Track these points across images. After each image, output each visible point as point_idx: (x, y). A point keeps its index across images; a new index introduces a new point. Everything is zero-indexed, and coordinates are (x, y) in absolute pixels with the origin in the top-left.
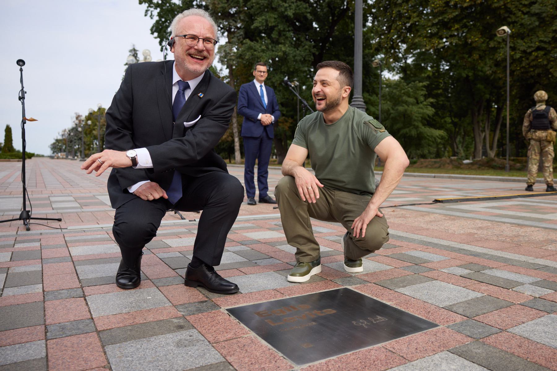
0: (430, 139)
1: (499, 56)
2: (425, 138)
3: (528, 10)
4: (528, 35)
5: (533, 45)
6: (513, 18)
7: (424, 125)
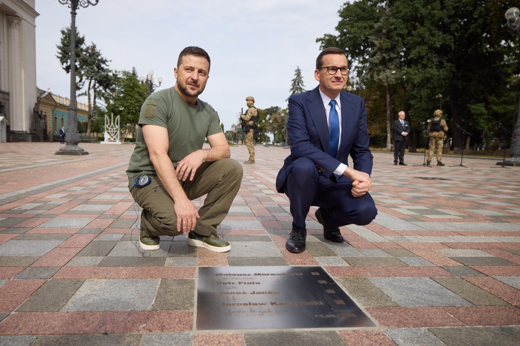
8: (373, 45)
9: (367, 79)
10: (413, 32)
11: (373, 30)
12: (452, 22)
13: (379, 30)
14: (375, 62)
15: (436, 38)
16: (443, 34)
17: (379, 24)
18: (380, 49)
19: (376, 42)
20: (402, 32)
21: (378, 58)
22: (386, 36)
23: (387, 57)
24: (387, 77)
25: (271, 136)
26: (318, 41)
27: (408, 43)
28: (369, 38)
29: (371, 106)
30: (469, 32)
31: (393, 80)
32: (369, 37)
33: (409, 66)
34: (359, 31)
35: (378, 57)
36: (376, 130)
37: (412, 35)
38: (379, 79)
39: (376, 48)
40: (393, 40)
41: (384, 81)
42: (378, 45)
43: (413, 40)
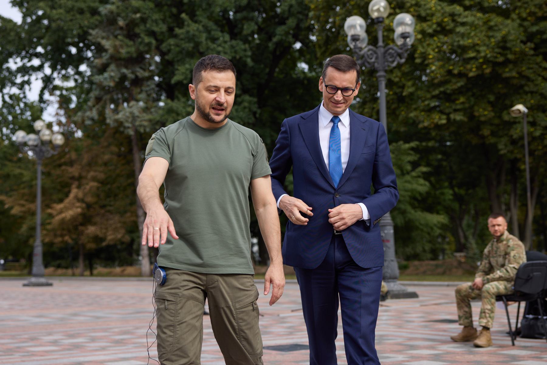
0: (425, 229)
1: (515, 133)
2: (417, 228)
7: (414, 207)
8: (100, 50)
9: (92, 119)
10: (177, 31)
11: (98, 18)
12: (246, 19)
13: (111, 21)
14: (106, 83)
15: (219, 45)
16: (231, 39)
17: (109, 6)
18: (116, 59)
19: (106, 44)
20: (155, 29)
21: (111, 77)
22: (125, 32)
23: (131, 76)
24: (134, 118)
27: (169, 51)
28: (91, 35)
29: (101, 176)
30: (275, 39)
31: (146, 123)
32: (91, 31)
33: (171, 96)
34: (69, 17)
35: (112, 74)
36: (116, 230)
37: (176, 36)
38: (116, 121)
39: (105, 57)
40: (141, 43)
41: (127, 125)
42: (111, 51)
43: (177, 45)
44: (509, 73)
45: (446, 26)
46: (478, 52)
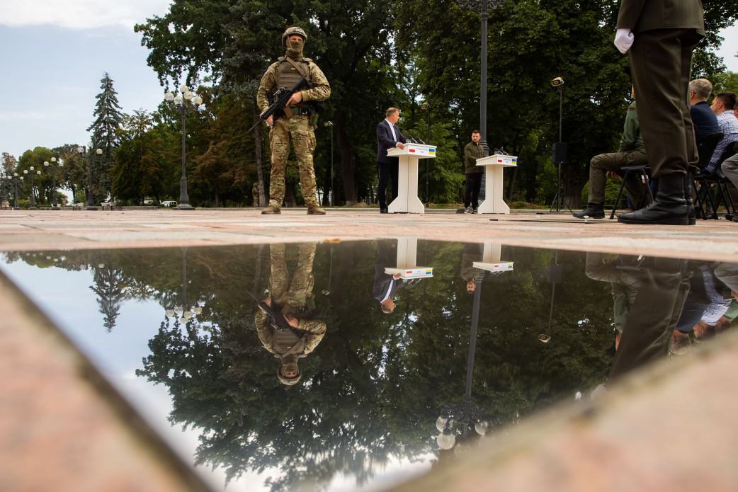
3: (575, 58)
4: (575, 84)
5: (580, 93)
6: (562, 67)
25: (68, 194)
26: (137, 29)
44: (548, 52)
45: (503, 13)
46: (528, 35)
